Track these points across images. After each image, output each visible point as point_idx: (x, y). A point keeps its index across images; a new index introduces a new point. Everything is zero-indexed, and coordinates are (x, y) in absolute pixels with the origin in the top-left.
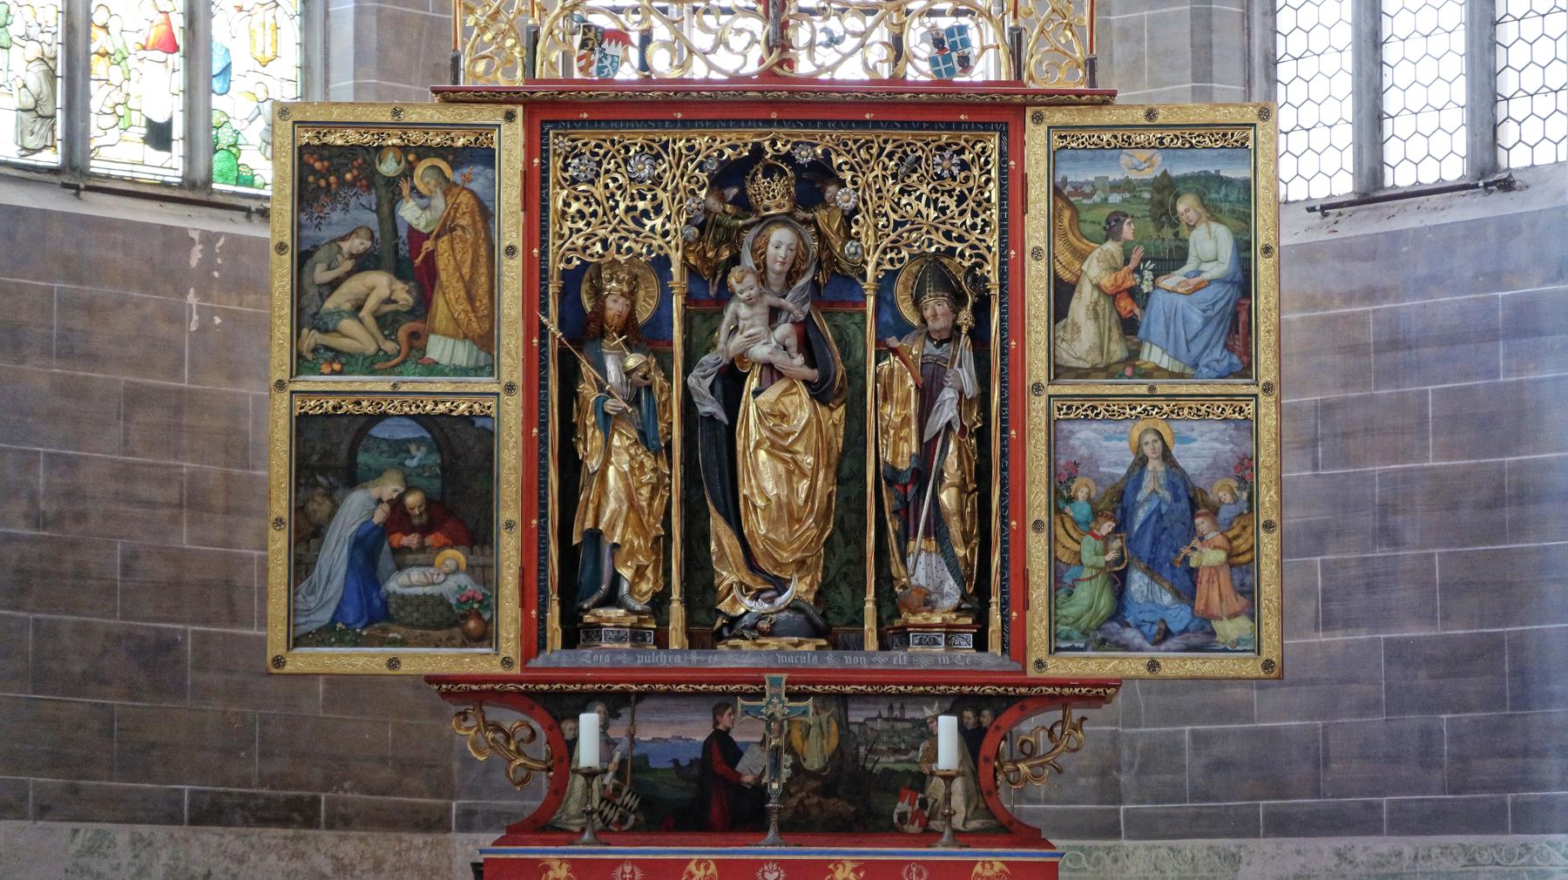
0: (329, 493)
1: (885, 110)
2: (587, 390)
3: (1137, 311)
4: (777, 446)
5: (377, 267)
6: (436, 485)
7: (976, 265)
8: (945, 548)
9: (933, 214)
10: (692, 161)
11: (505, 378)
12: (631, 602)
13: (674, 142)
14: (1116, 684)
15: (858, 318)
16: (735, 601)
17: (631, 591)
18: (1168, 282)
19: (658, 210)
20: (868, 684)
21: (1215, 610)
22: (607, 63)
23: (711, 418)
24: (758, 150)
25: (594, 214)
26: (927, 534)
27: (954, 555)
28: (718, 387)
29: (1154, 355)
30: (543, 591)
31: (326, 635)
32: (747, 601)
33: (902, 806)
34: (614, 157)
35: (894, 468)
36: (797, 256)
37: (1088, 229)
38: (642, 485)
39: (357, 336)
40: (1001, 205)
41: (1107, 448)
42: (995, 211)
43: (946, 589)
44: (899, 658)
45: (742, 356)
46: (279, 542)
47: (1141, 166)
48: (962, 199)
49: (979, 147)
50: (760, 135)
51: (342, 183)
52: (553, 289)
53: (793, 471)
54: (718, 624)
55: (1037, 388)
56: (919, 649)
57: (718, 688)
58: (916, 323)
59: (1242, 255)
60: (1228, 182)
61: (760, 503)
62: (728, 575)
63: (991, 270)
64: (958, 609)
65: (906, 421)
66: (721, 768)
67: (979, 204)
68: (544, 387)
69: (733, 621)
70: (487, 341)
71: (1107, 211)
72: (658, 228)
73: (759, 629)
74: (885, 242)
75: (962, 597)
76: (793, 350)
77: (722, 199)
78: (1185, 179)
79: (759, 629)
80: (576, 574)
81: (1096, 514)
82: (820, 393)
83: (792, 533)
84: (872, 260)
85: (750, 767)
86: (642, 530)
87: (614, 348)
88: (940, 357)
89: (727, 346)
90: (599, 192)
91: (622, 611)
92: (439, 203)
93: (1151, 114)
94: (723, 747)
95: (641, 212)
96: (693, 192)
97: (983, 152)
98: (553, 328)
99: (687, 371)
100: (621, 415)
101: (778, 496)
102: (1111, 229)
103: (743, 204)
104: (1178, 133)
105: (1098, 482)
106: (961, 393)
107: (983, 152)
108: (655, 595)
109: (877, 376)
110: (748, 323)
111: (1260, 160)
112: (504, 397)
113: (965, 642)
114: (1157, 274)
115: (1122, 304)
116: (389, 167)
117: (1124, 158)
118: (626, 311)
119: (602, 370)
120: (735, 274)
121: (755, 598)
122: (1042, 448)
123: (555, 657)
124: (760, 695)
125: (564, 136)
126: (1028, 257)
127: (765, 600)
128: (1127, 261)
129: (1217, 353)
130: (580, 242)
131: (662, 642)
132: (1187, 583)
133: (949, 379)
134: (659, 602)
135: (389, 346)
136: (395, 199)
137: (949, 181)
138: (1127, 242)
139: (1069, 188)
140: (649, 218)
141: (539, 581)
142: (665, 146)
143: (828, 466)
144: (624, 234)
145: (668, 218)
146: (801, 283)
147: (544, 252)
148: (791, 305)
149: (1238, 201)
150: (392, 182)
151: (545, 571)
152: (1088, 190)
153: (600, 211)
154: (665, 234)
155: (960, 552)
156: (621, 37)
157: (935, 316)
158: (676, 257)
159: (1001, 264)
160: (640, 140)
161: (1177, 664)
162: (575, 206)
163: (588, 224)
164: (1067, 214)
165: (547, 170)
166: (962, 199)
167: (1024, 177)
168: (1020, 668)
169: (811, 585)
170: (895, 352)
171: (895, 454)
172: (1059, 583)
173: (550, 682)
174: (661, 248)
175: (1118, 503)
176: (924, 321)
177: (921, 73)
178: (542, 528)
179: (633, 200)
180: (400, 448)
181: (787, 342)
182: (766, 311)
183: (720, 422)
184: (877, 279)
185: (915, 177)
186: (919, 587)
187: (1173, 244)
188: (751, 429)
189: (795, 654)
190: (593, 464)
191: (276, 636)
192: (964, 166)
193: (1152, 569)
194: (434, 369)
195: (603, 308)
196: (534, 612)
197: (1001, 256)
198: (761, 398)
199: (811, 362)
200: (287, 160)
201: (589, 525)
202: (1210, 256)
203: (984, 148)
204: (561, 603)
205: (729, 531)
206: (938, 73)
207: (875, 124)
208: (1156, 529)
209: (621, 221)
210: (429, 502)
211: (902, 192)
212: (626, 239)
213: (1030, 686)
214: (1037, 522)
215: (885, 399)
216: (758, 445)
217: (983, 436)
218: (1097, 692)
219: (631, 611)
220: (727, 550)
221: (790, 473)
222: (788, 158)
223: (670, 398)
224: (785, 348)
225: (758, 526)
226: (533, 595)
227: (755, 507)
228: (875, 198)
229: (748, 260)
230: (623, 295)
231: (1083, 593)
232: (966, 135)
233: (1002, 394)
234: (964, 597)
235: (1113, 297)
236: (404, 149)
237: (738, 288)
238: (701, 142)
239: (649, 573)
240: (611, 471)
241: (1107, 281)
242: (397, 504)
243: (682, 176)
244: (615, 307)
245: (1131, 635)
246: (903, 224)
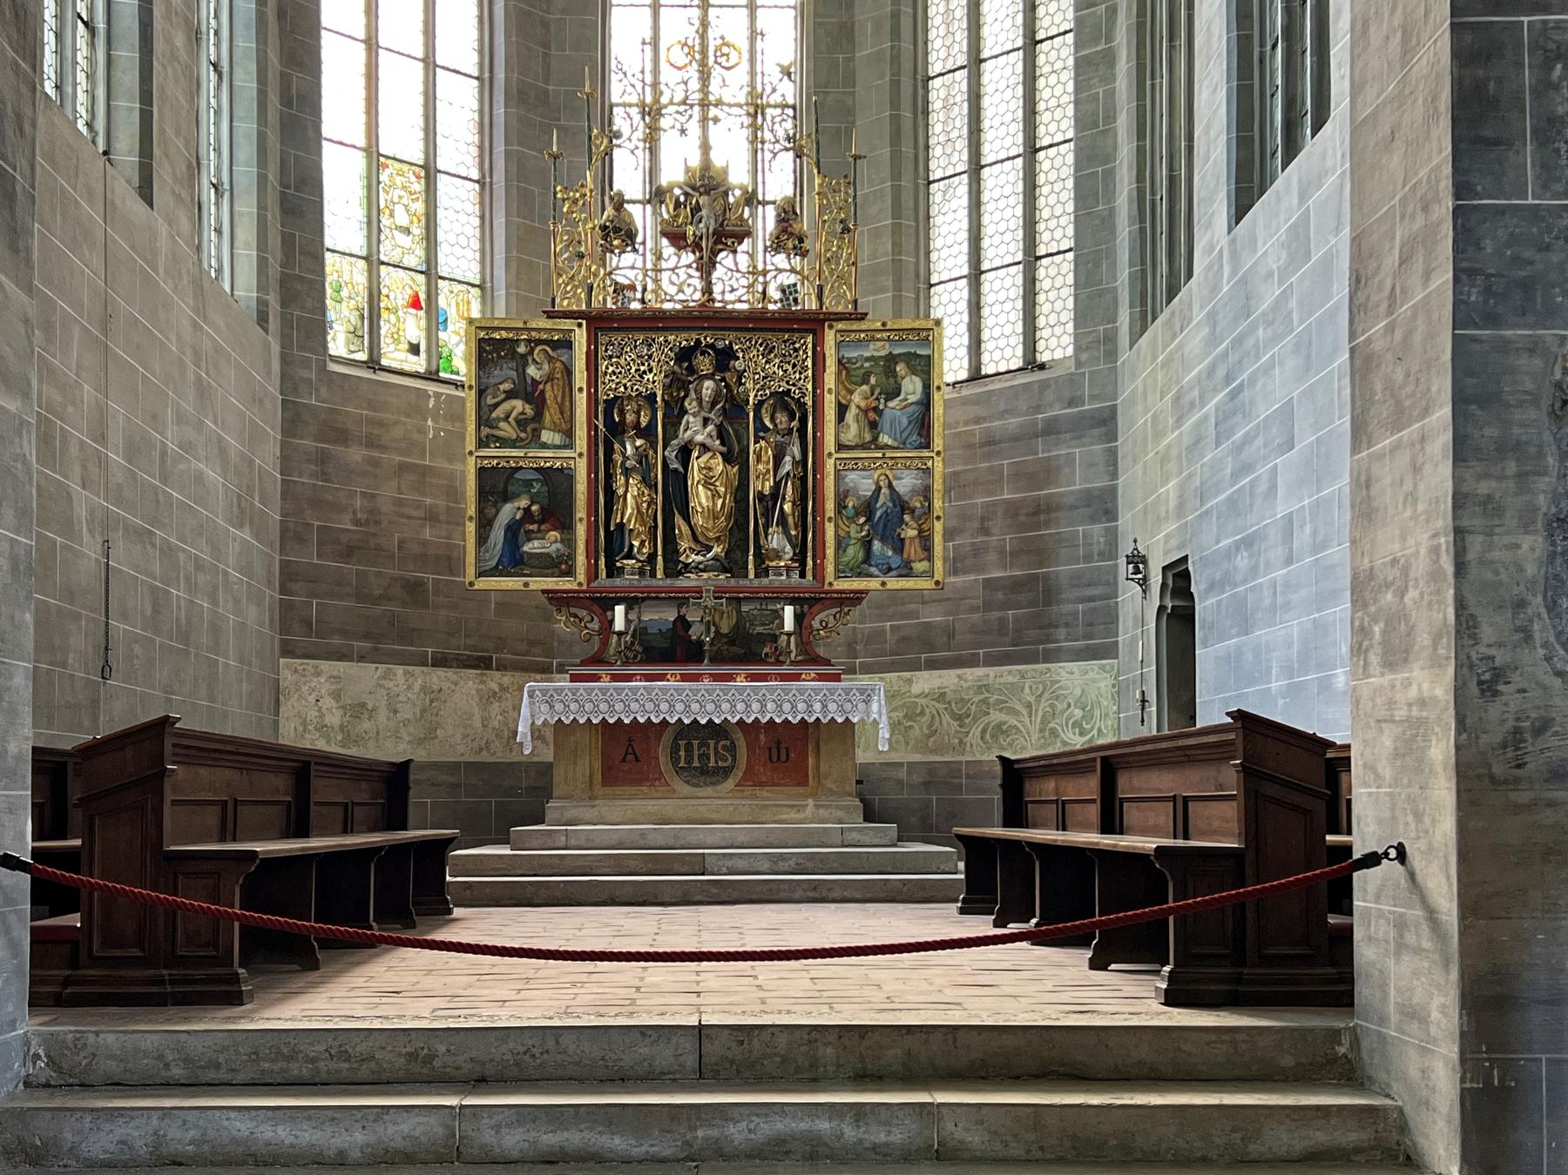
0: (495, 505)
1: (756, 322)
2: (618, 458)
5: (516, 398)
6: (546, 501)
8: (786, 533)
14: (866, 592)
18: (891, 404)
19: (651, 371)
21: (912, 556)
24: (698, 342)
29: (885, 439)
30: (597, 551)
31: (494, 572)
33: (766, 650)
39: (507, 430)
41: (863, 483)
42: (810, 372)
45: (690, 441)
46: (471, 528)
47: (879, 350)
51: (499, 357)
53: (716, 495)
55: (830, 455)
62: (684, 545)
63: (809, 400)
66: (682, 633)
69: (687, 565)
70: (569, 433)
73: (698, 569)
79: (698, 569)
80: (613, 543)
81: (857, 514)
82: (727, 458)
84: (752, 395)
85: (694, 633)
86: (643, 523)
90: (622, 361)
92: (546, 366)
93: (884, 324)
94: (683, 623)
95: (642, 370)
100: (633, 469)
102: (865, 381)
103: (691, 370)
105: (858, 498)
113: (796, 575)
114: (886, 400)
116: (522, 349)
117: (872, 346)
131: (653, 574)
132: (899, 545)
134: (652, 558)
135: (523, 435)
136: (525, 365)
150: (523, 356)
156: (633, 288)
161: (894, 583)
166: (794, 366)
172: (840, 545)
175: (868, 508)
178: (597, 521)
180: (528, 484)
188: (695, 474)
190: (621, 491)
191: (471, 571)
192: (796, 350)
193: (883, 540)
194: (544, 446)
199: (723, 444)
200: (473, 345)
207: (753, 330)
208: (888, 524)
210: (542, 508)
213: (827, 592)
217: (804, 479)
218: (856, 598)
222: (712, 346)
225: (699, 520)
226: (592, 553)
231: (851, 551)
235: (866, 412)
236: (529, 341)
238: (671, 338)
241: (863, 404)
242: (527, 510)
244: (630, 418)
245: (873, 570)
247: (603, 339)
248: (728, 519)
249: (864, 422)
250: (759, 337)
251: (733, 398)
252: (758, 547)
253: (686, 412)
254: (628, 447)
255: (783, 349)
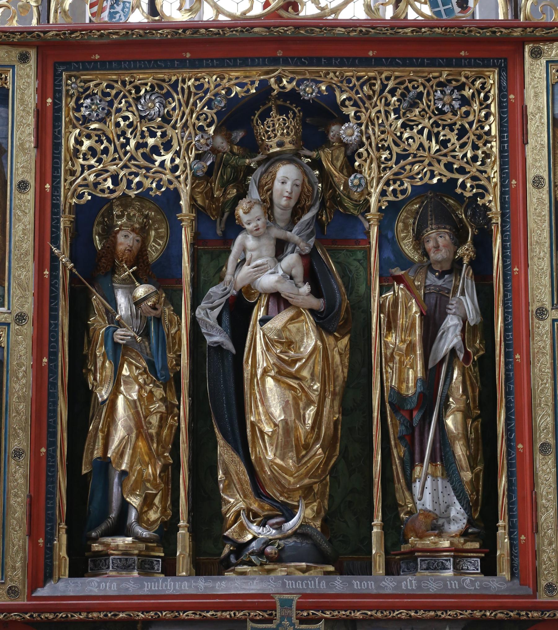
2: (98, 323)
4: (284, 372)
7: (476, 195)
9: (435, 147)
10: (201, 99)
11: (16, 310)
12: (139, 530)
13: (184, 81)
15: (360, 255)
16: (243, 529)
17: (139, 520)
19: (168, 146)
20: (378, 608)
22: (119, 8)
23: (219, 348)
25: (106, 151)
26: (433, 460)
27: (460, 480)
28: (226, 319)
30: (51, 520)
32: (254, 528)
34: (125, 96)
35: (399, 394)
36: (302, 192)
38: (151, 413)
40: (501, 137)
42: (495, 144)
43: (453, 513)
44: (408, 583)
48: (462, 132)
49: (478, 83)
50: (267, 73)
52: (64, 222)
54: (226, 551)
55: (541, 312)
56: (427, 573)
57: (226, 615)
58: (416, 258)
61: (268, 429)
62: (234, 502)
64: (464, 534)
65: (411, 347)
67: (479, 137)
68: (54, 317)
69: (241, 548)
72: (168, 164)
74: (388, 174)
75: (469, 521)
76: (299, 277)
77: (230, 142)
82: (324, 322)
83: (299, 459)
87: (124, 281)
88: (441, 288)
89: (237, 277)
91: (129, 540)
96: (201, 128)
97: (483, 88)
98: (64, 259)
99: (195, 304)
101: (285, 421)
103: (252, 145)
106: (465, 320)
107: (483, 88)
108: (164, 524)
109: (381, 307)
110: (255, 254)
112: (14, 327)
113: (473, 565)
118: (136, 246)
119: (115, 305)
120: (243, 204)
121: (263, 524)
122: (548, 370)
123: (61, 584)
124: (270, 621)
125: (77, 78)
126: (529, 185)
127: (272, 526)
130: (92, 178)
131: (169, 569)
133: (453, 306)
134: (166, 533)
137: (450, 115)
140: (159, 155)
141: (47, 509)
142: (175, 86)
143: (334, 394)
144: (134, 169)
145: (178, 153)
146: (307, 217)
147: (56, 188)
148: (297, 238)
151: (54, 499)
153: (112, 149)
154: (175, 169)
155: (467, 476)
157: (437, 247)
158: (185, 192)
159: (502, 193)
160: (150, 81)
162: (87, 143)
163: (99, 161)
165: (60, 109)
166: (462, 132)
167: (524, 109)
168: (530, 591)
169: (318, 512)
170: (399, 280)
171: (401, 381)
173: (54, 610)
174: (170, 182)
176: (426, 254)
177: (421, 14)
178: (51, 455)
179: (143, 136)
181: (294, 272)
182: (273, 242)
183: (228, 351)
184: (380, 209)
185: (417, 111)
186: (426, 513)
188: (260, 355)
189: (303, 580)
190: (103, 394)
192: (465, 101)
195: (114, 244)
196: (41, 541)
197: (502, 186)
198: (268, 325)
199: (316, 292)
201: (97, 453)
203: (484, 84)
204: (67, 532)
205: (237, 459)
206: (438, 13)
207: (377, 62)
209: (132, 158)
211: (404, 126)
212: (136, 175)
213: (543, 608)
214: (542, 445)
215: (389, 329)
216: (265, 372)
217: (486, 365)
219: (139, 539)
220: (235, 478)
221: (296, 399)
223: (179, 329)
224: (292, 278)
227: (262, 432)
228: (378, 133)
229: (254, 194)
230: (133, 230)
232: (467, 71)
233: (505, 319)
234: (471, 522)
237: (245, 218)
238: (210, 80)
239: (157, 501)
240: (121, 401)
243: (192, 112)
244: (125, 241)
246: (405, 157)
247: (70, 84)
248: (328, 447)
250: (392, 75)
251: (336, 200)
252: (391, 507)
253: (240, 229)
254: (122, 300)
255: (440, 99)
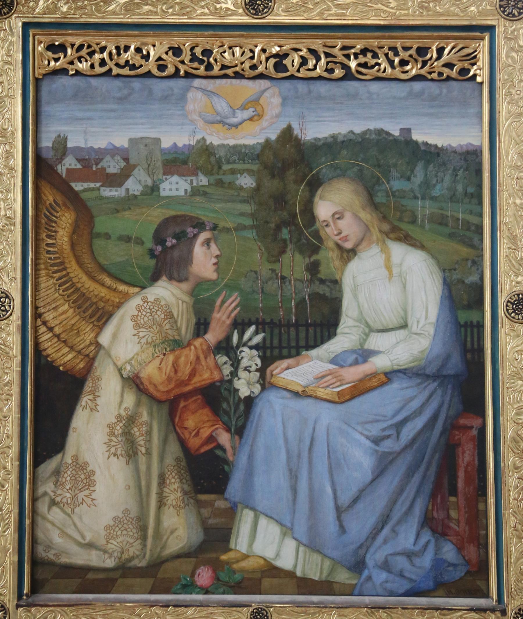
3: (224, 438)
18: (303, 371)
29: (262, 540)
37: (113, 253)
59: (463, 316)
60: (431, 155)
71: (157, 215)
78: (332, 146)
102: (166, 259)
104: (317, 44)
111: (503, 108)
114: (270, 355)
115: (191, 422)
117: (198, 97)
128: (202, 326)
129: (407, 537)
138: (201, 284)
139: (70, 163)
149: (453, 198)
152: (113, 166)
164: (66, 219)
187: (306, 293)
202: (391, 318)
235: (171, 405)
241: (154, 372)
249: (161, 455)
